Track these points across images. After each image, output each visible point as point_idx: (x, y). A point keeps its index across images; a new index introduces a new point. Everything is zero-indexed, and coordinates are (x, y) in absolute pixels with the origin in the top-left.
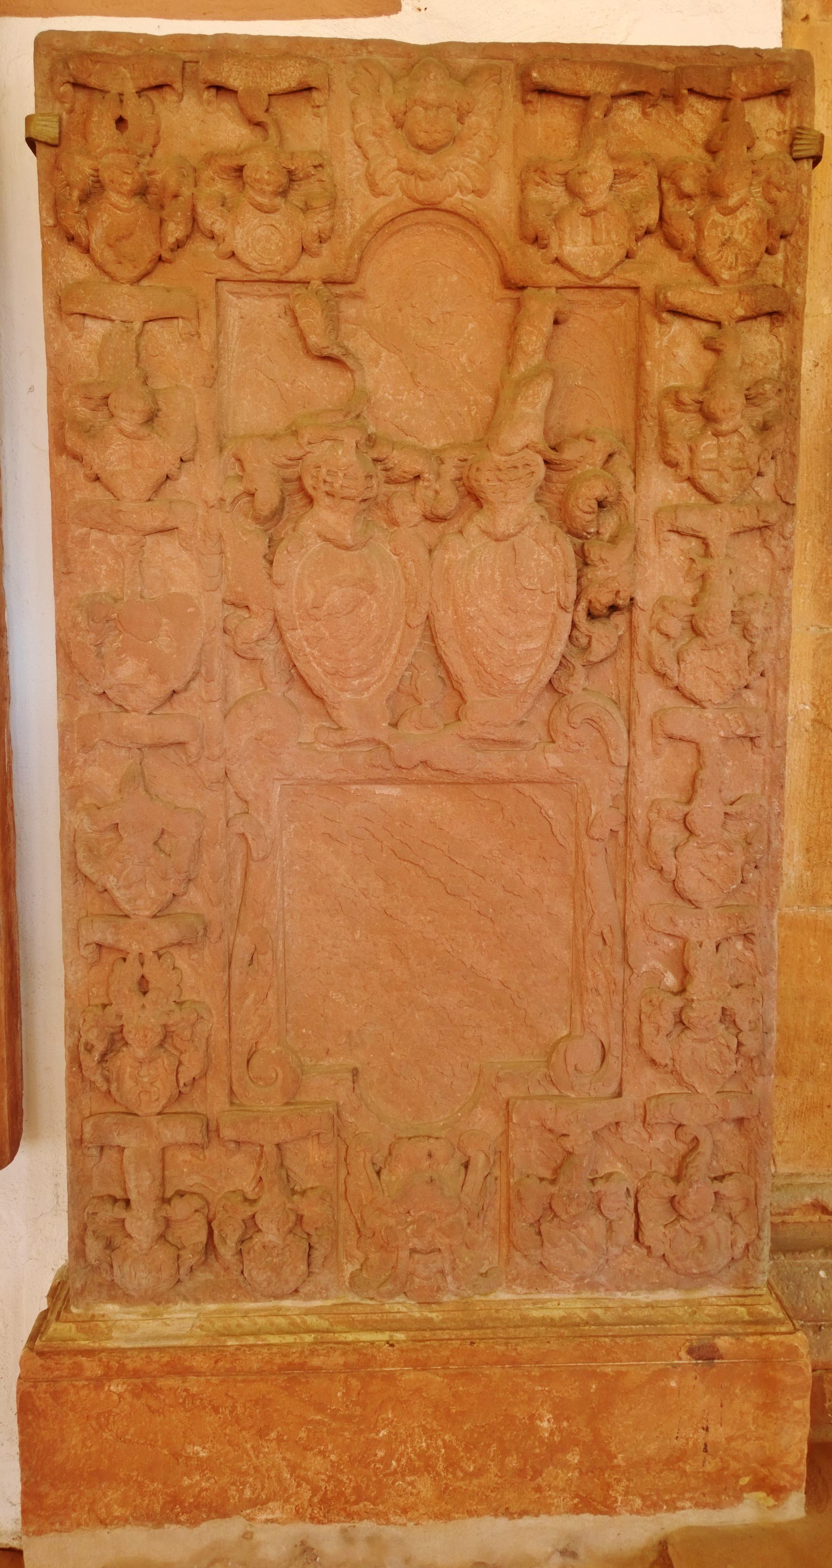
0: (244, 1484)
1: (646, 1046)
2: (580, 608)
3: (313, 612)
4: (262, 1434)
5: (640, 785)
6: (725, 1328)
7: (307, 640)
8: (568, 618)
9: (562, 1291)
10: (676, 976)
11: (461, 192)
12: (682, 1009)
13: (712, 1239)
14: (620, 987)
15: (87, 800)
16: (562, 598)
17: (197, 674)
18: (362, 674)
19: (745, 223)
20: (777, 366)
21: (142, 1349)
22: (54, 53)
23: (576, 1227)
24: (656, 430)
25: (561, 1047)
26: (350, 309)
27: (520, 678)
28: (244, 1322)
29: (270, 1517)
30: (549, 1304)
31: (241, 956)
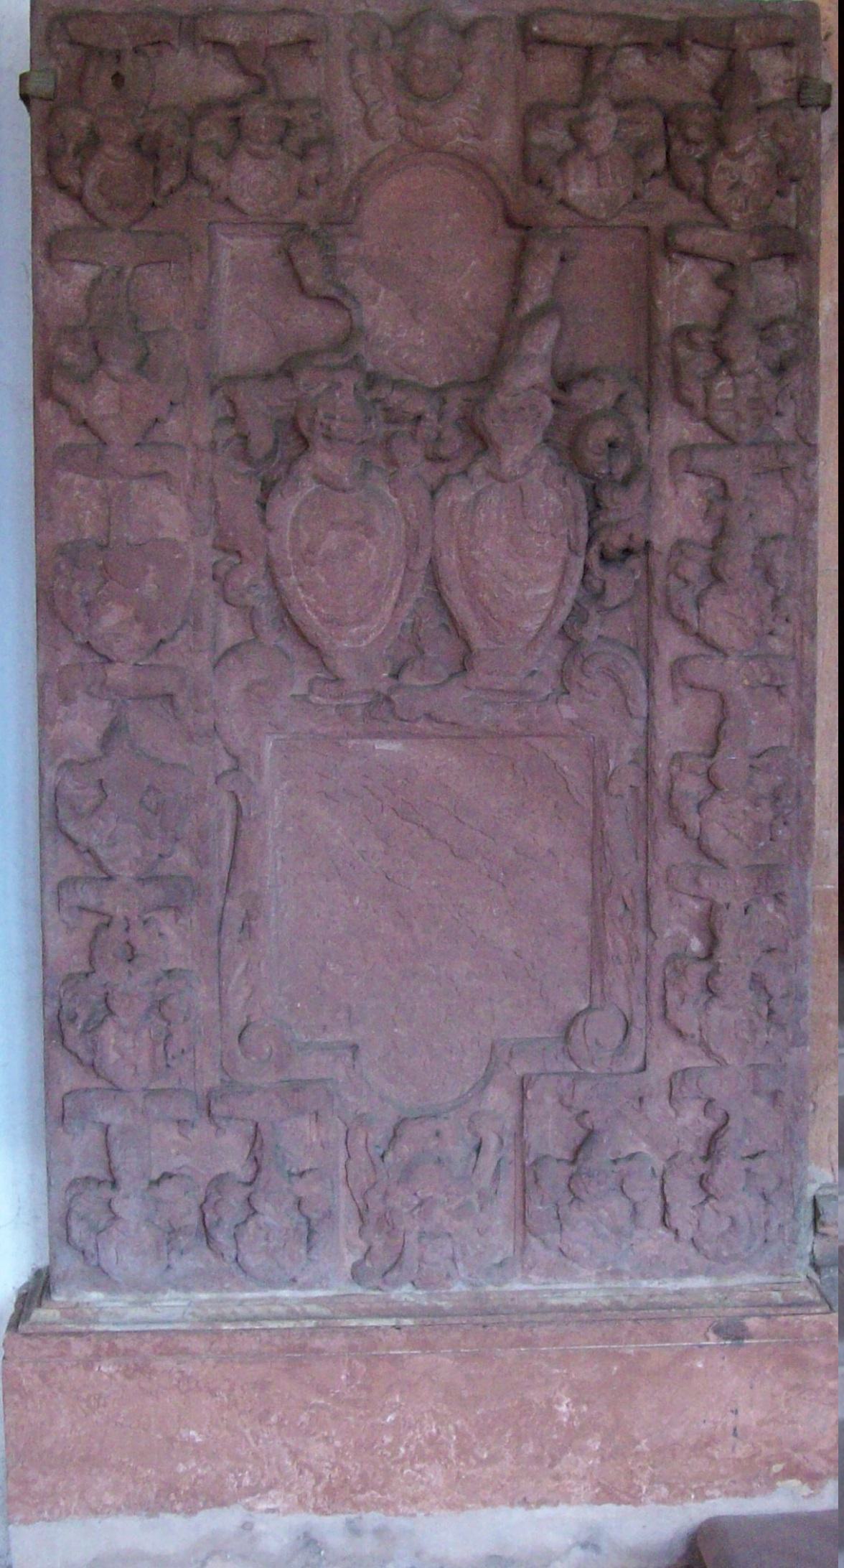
0: (242, 1470)
1: (670, 1014)
2: (592, 551)
4: (263, 1418)
7: (301, 586)
8: (581, 561)
11: (463, 136)
12: (709, 977)
13: (743, 1220)
14: (642, 952)
15: (67, 756)
16: (573, 543)
18: (360, 621)
23: (597, 1209)
25: (581, 1021)
29: (272, 1506)
31: (234, 922)
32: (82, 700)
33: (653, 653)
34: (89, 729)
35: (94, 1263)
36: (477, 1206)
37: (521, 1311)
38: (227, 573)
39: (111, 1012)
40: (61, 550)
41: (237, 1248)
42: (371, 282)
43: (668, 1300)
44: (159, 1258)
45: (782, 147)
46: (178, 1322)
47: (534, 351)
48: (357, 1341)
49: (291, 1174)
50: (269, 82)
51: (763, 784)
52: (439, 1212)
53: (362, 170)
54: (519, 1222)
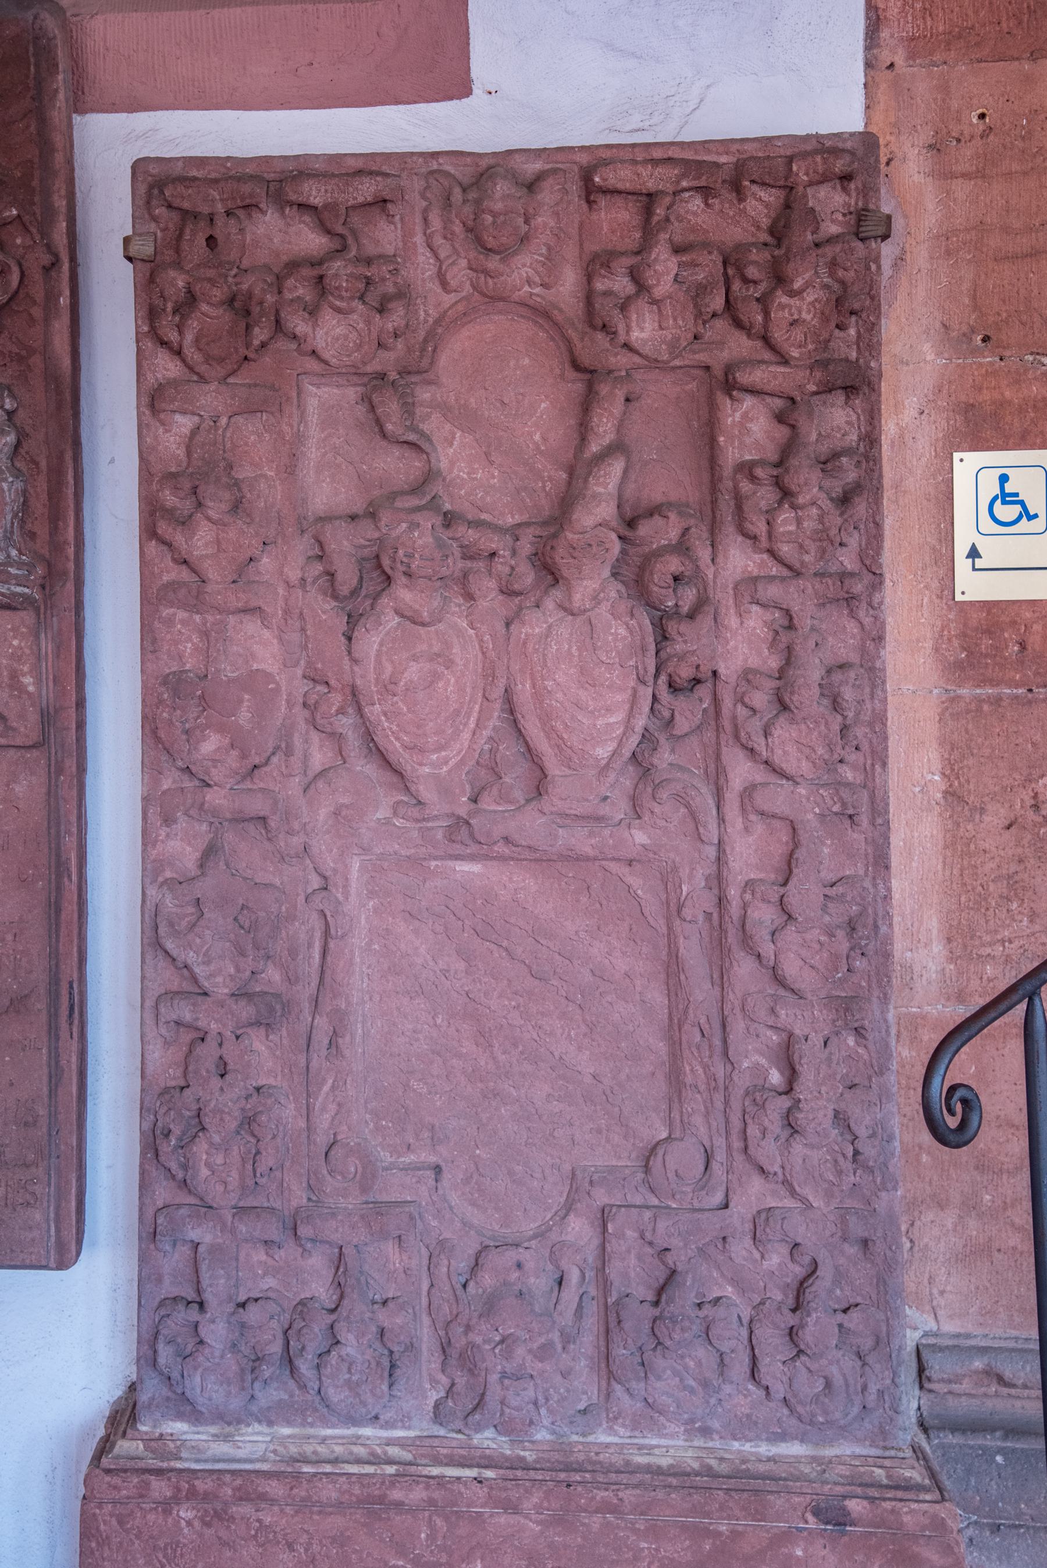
1: (752, 1151)
2: (660, 682)
3: (391, 687)
5: (731, 864)
6: (859, 1490)
7: (385, 714)
8: (649, 691)
9: (672, 1436)
10: (782, 1073)
11: (530, 285)
12: (789, 1111)
13: (838, 1381)
14: (721, 1082)
16: (642, 672)
17: (277, 748)
18: (440, 748)
19: (812, 303)
20: (855, 438)
21: (212, 1472)
22: (150, 178)
23: (682, 1357)
24: (732, 503)
25: (660, 1152)
26: (425, 394)
27: (603, 752)
28: (319, 1449)
30: (656, 1451)
31: (321, 1039)
32: (182, 822)
33: (722, 780)
34: (189, 849)
35: (179, 1391)
36: (559, 1347)
37: (609, 1469)
38: (317, 702)
39: (203, 1129)
40: (165, 681)
41: (320, 1379)
42: (448, 426)
43: (762, 1468)
44: (243, 1389)
45: (842, 282)
46: (258, 1460)
47: (601, 490)
48: (437, 1495)
49: (374, 1303)
50: (350, 241)
51: (837, 914)
52: (520, 1351)
53: (438, 322)
54: (603, 1365)
